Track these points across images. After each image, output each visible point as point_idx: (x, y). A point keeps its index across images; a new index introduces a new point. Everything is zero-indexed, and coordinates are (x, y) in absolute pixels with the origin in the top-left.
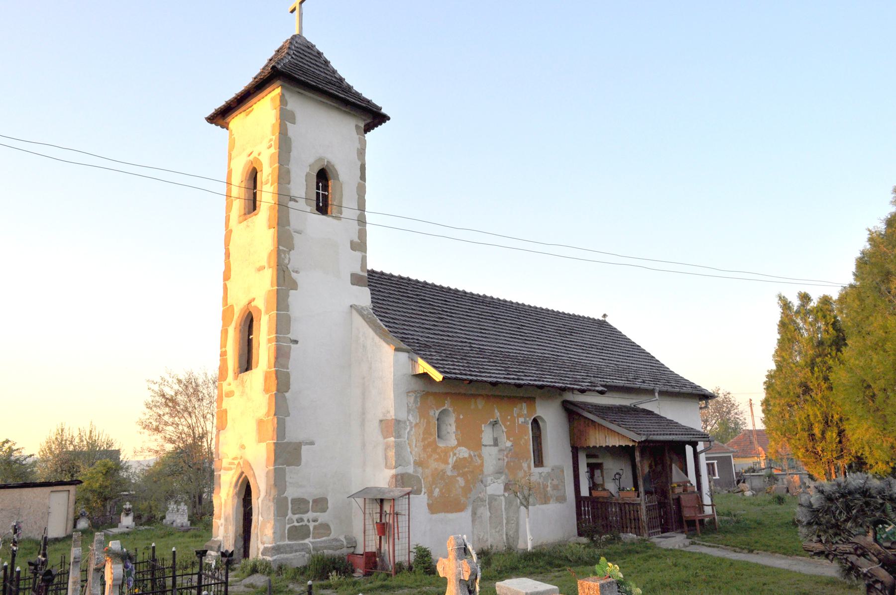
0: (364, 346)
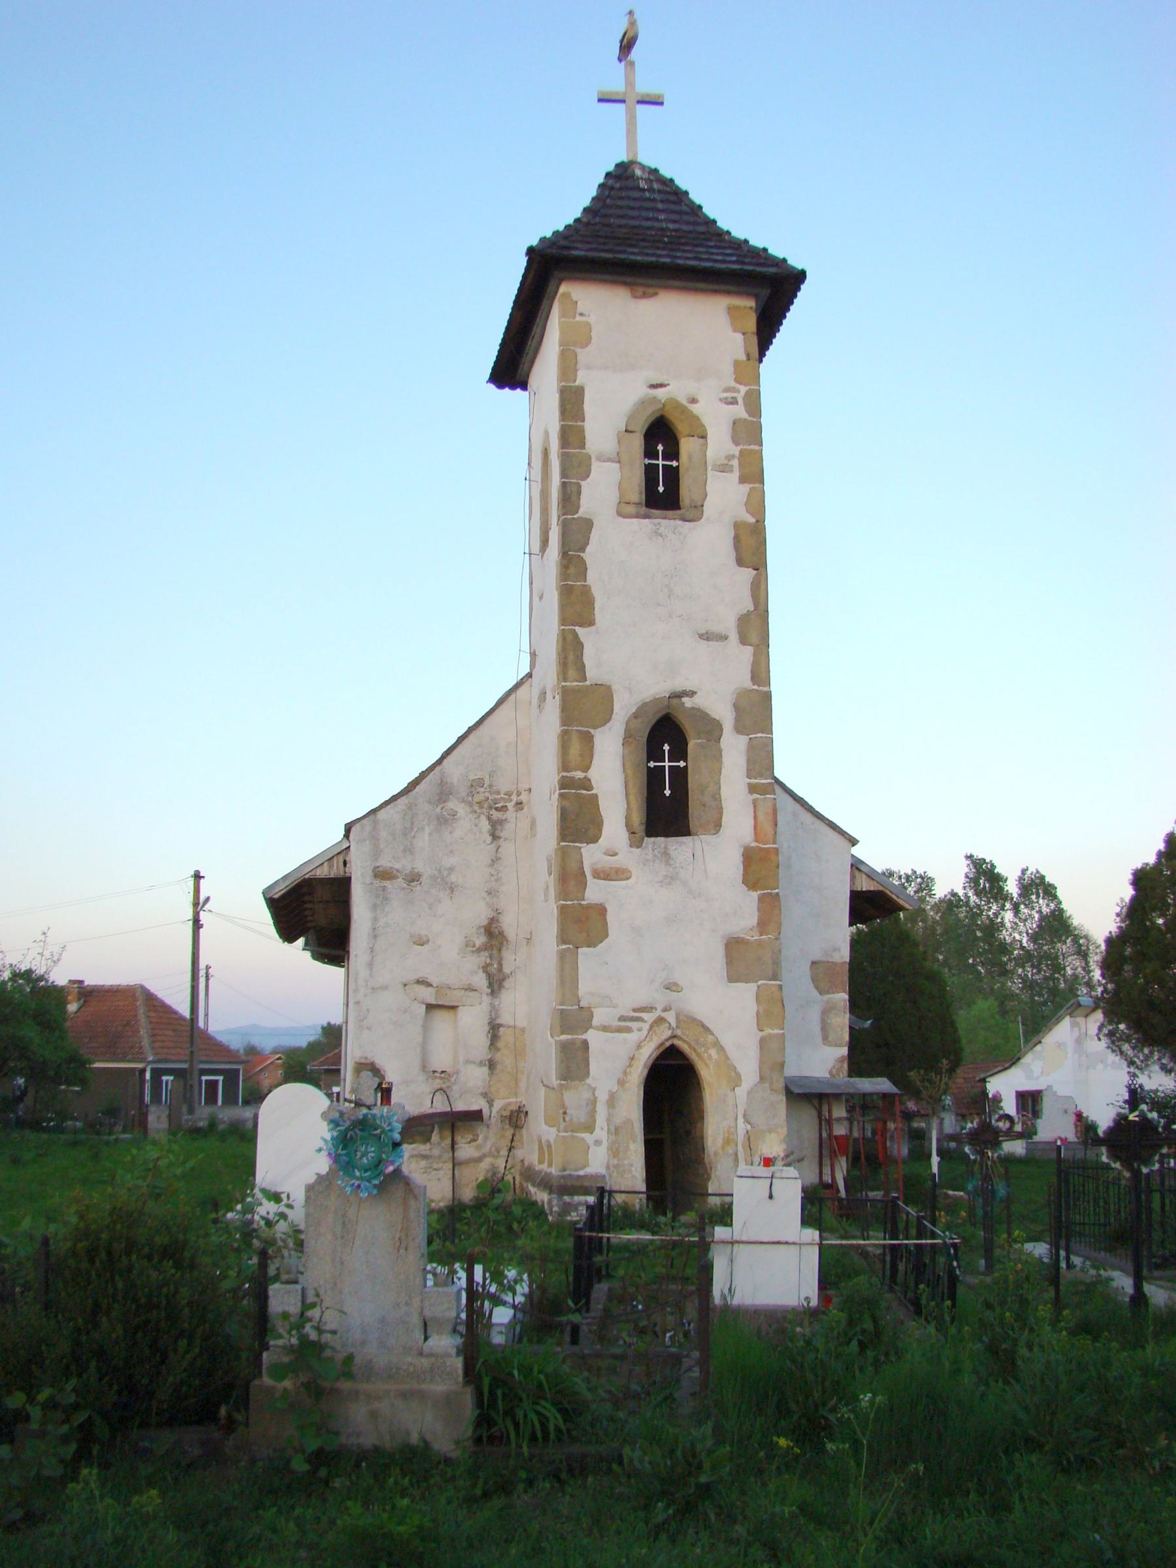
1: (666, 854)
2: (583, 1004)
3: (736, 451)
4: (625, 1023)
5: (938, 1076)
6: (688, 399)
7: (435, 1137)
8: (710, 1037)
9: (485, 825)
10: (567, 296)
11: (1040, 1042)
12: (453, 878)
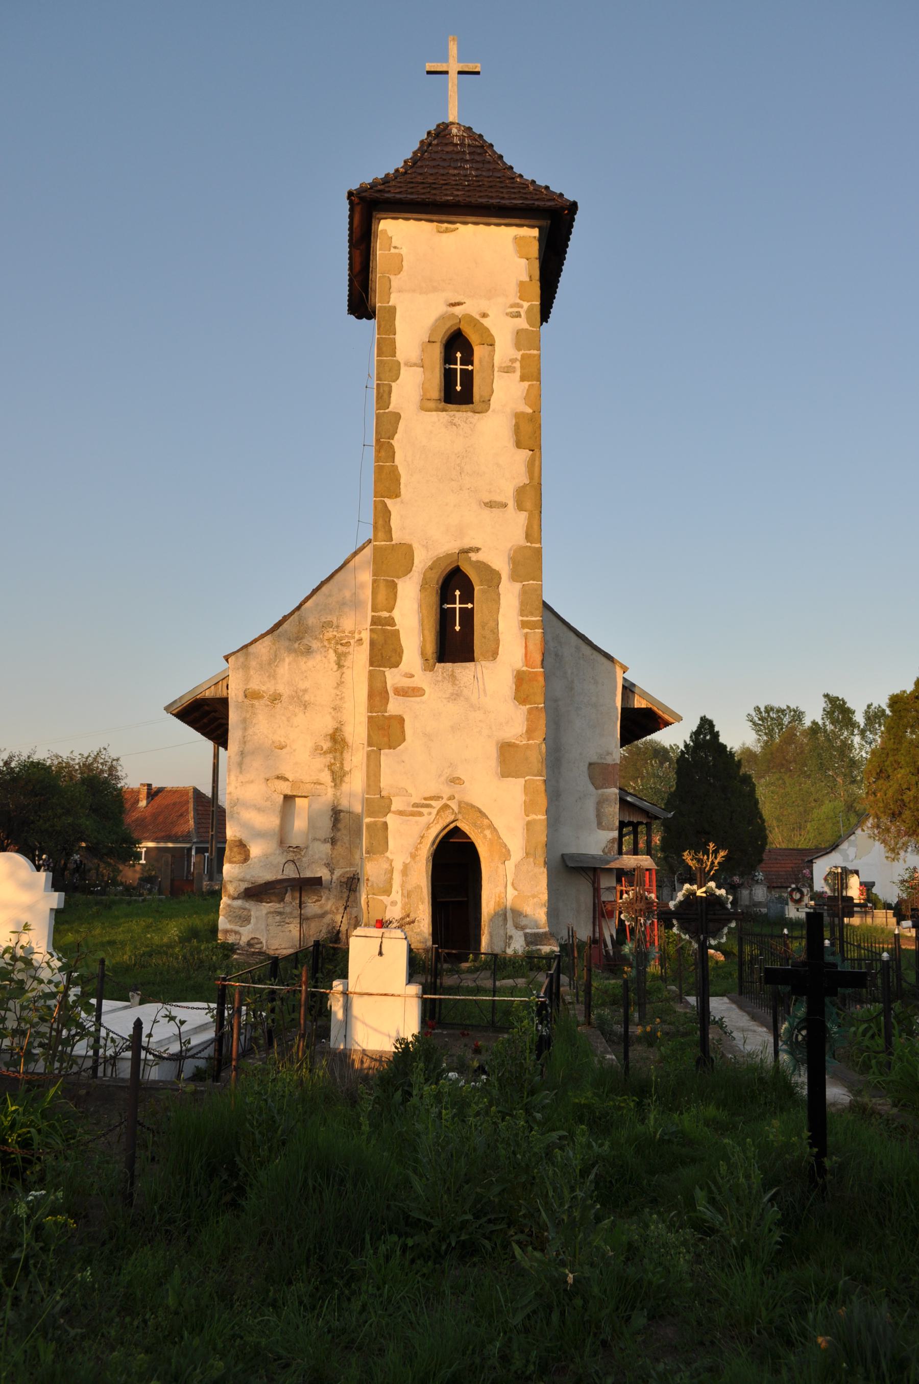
0: (557, 655)
1: (453, 677)
2: (383, 794)
3: (518, 355)
4: (415, 811)
5: (705, 857)
6: (480, 314)
7: (288, 898)
8: (486, 821)
9: (332, 656)
10: (384, 231)
11: (854, 833)
12: (307, 697)
